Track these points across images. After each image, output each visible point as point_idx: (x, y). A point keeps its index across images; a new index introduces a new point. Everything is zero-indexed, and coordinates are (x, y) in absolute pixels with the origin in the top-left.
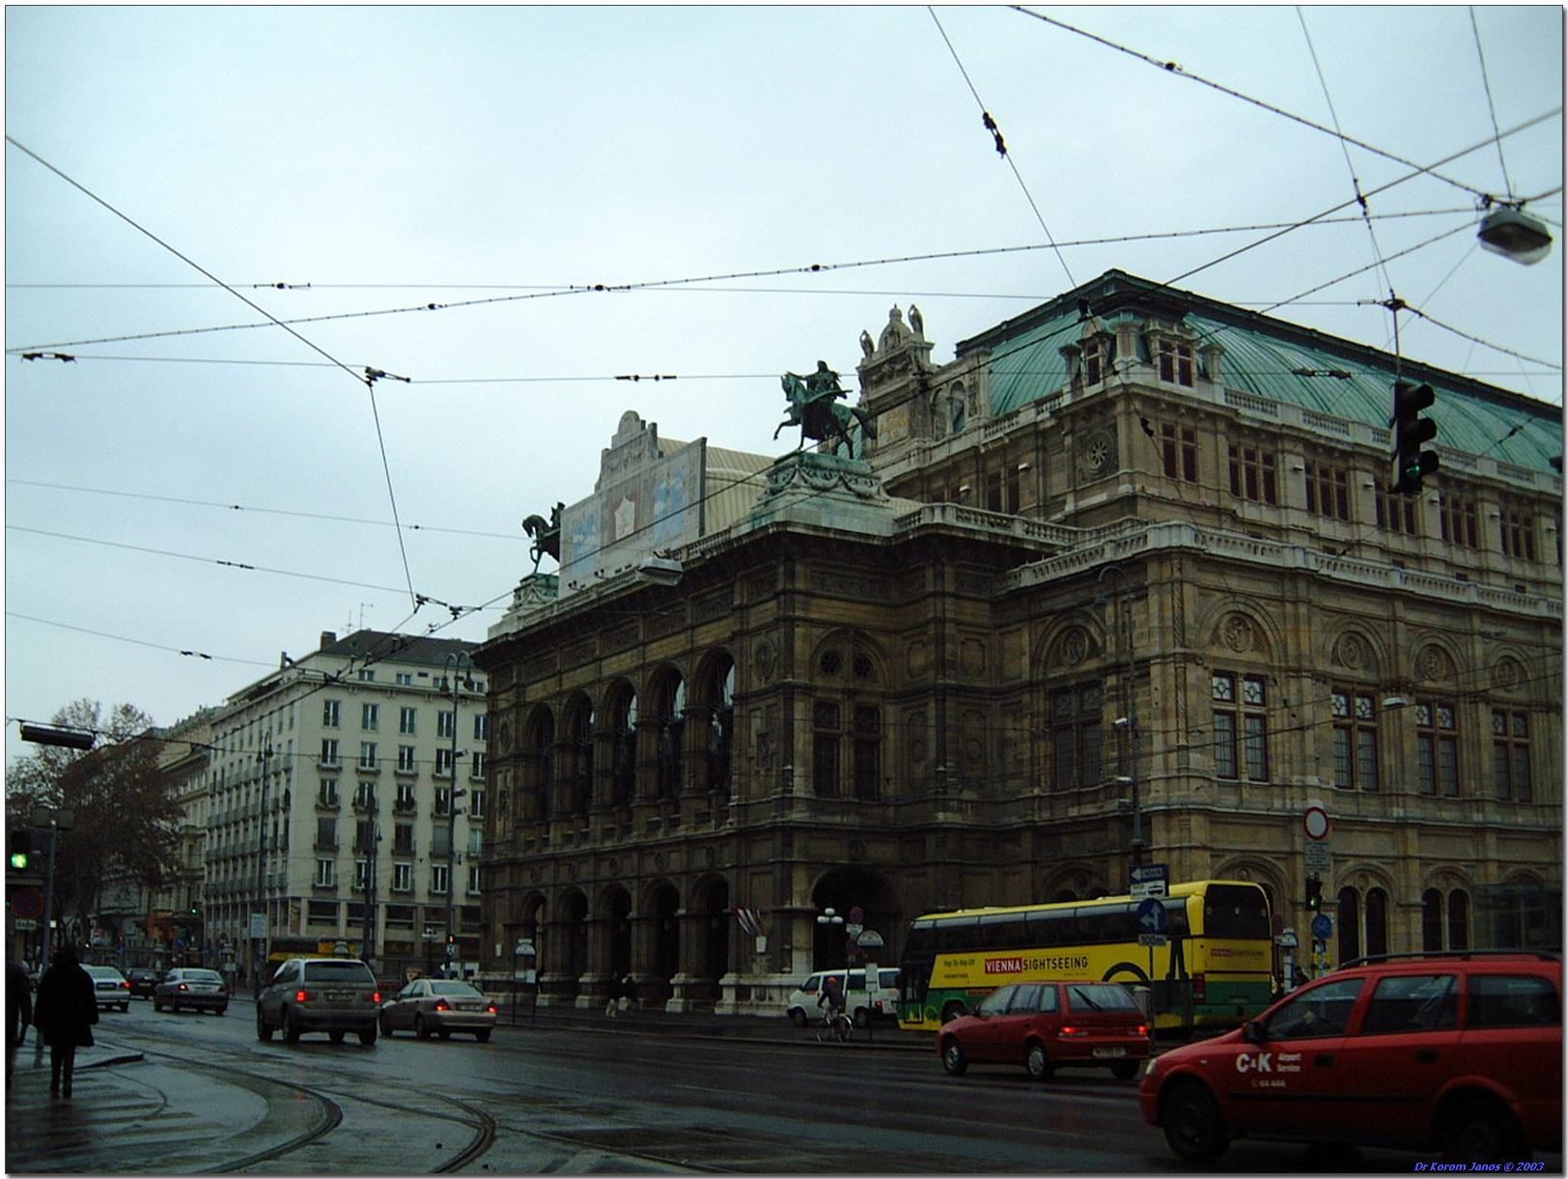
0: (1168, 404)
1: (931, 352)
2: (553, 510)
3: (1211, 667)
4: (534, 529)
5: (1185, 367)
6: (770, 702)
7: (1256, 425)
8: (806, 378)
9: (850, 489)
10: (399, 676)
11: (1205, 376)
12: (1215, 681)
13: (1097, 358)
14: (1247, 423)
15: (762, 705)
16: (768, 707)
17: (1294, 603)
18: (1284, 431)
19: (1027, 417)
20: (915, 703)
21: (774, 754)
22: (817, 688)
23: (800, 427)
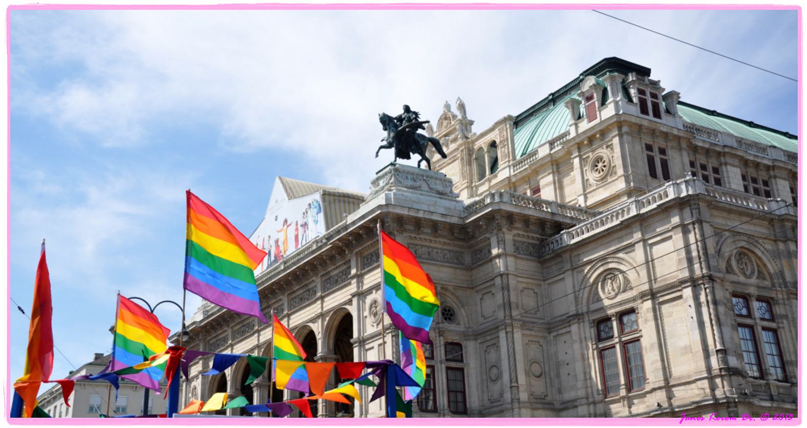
0: (648, 128)
1: (473, 127)
3: (731, 288)
5: (656, 107)
6: (381, 341)
7: (707, 146)
8: (395, 118)
9: (431, 189)
11: (668, 111)
12: (734, 300)
13: (594, 103)
14: (700, 144)
15: (375, 344)
16: (380, 345)
17: (784, 242)
18: (727, 150)
19: (544, 151)
20: (488, 338)
23: (393, 150)
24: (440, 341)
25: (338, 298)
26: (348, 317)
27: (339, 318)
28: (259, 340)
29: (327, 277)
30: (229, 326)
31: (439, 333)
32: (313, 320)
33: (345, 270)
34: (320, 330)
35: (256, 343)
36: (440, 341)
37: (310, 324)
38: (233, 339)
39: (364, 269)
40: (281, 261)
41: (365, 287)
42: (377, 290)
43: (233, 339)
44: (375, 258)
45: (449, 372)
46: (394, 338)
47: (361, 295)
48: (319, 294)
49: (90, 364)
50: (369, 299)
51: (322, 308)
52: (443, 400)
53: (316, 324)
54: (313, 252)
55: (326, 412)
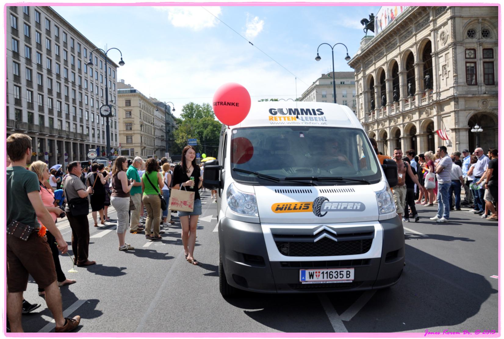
2: (370, 16)
4: (364, 23)
10: (341, 83)
15: (443, 54)
16: (446, 54)
21: (449, 71)
22: (466, 43)
24: (480, 48)
25: (423, 34)
26: (429, 43)
27: (424, 44)
28: (386, 59)
29: (418, 24)
30: (372, 55)
31: (480, 44)
32: (412, 47)
33: (427, 19)
34: (415, 51)
35: (385, 61)
36: (480, 48)
37: (410, 49)
38: (375, 60)
39: (437, 16)
40: (394, 20)
41: (438, 26)
42: (444, 26)
43: (375, 60)
44: (443, 9)
45: (485, 64)
46: (453, 50)
47: (435, 30)
48: (414, 33)
49: (320, 78)
50: (440, 32)
51: (416, 40)
52: (480, 78)
53: (413, 48)
54: (410, 12)
55: (420, 89)
